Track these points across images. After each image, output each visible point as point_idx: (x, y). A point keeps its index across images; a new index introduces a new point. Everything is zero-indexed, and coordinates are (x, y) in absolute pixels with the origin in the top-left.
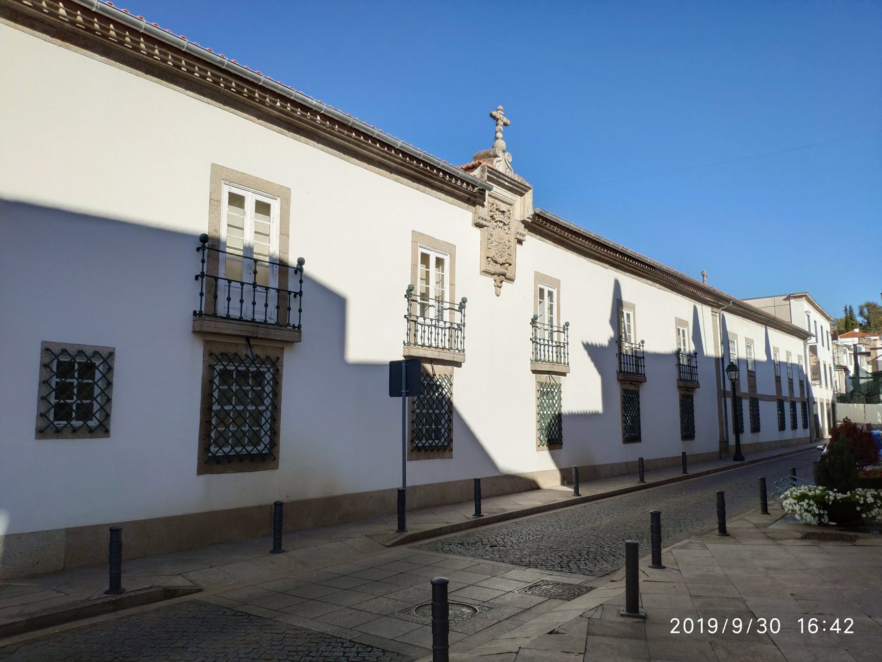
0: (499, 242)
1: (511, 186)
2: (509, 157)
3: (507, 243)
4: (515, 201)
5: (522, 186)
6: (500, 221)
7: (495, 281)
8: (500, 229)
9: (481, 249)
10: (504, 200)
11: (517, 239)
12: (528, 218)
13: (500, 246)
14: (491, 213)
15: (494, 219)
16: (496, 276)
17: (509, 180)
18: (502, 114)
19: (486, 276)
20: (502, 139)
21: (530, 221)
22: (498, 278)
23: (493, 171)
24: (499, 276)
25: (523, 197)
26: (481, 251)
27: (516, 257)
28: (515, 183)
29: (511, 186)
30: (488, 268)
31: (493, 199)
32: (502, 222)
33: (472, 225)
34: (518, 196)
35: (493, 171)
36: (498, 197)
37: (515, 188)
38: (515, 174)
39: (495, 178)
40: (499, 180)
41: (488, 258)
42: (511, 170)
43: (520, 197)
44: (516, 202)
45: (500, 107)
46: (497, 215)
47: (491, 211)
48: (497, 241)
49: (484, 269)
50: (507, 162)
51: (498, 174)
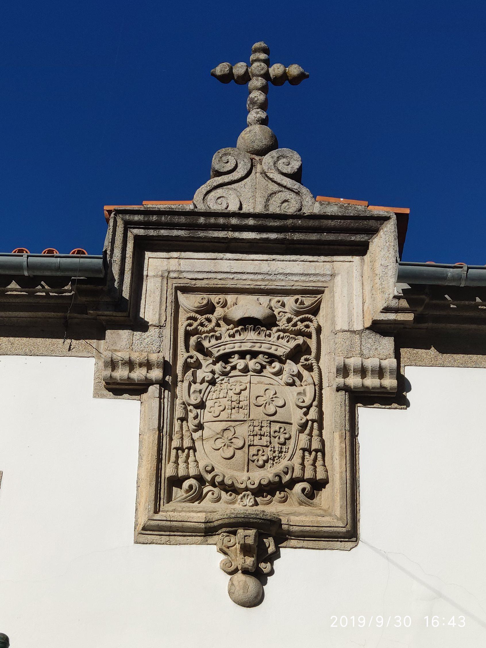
0: (233, 417)
1: (273, 236)
4: (333, 275)
5: (332, 223)
6: (242, 355)
10: (262, 285)
11: (345, 388)
15: (206, 353)
17: (251, 222)
21: (410, 317)
23: (154, 218)
28: (290, 222)
29: (273, 236)
32: (254, 354)
33: (97, 395)
34: (349, 258)
35: (154, 218)
36: (229, 284)
37: (297, 236)
39: (181, 233)
40: (202, 234)
42: (298, 193)
43: (356, 259)
44: (338, 279)
48: (224, 416)
50: (279, 178)
51: (183, 220)
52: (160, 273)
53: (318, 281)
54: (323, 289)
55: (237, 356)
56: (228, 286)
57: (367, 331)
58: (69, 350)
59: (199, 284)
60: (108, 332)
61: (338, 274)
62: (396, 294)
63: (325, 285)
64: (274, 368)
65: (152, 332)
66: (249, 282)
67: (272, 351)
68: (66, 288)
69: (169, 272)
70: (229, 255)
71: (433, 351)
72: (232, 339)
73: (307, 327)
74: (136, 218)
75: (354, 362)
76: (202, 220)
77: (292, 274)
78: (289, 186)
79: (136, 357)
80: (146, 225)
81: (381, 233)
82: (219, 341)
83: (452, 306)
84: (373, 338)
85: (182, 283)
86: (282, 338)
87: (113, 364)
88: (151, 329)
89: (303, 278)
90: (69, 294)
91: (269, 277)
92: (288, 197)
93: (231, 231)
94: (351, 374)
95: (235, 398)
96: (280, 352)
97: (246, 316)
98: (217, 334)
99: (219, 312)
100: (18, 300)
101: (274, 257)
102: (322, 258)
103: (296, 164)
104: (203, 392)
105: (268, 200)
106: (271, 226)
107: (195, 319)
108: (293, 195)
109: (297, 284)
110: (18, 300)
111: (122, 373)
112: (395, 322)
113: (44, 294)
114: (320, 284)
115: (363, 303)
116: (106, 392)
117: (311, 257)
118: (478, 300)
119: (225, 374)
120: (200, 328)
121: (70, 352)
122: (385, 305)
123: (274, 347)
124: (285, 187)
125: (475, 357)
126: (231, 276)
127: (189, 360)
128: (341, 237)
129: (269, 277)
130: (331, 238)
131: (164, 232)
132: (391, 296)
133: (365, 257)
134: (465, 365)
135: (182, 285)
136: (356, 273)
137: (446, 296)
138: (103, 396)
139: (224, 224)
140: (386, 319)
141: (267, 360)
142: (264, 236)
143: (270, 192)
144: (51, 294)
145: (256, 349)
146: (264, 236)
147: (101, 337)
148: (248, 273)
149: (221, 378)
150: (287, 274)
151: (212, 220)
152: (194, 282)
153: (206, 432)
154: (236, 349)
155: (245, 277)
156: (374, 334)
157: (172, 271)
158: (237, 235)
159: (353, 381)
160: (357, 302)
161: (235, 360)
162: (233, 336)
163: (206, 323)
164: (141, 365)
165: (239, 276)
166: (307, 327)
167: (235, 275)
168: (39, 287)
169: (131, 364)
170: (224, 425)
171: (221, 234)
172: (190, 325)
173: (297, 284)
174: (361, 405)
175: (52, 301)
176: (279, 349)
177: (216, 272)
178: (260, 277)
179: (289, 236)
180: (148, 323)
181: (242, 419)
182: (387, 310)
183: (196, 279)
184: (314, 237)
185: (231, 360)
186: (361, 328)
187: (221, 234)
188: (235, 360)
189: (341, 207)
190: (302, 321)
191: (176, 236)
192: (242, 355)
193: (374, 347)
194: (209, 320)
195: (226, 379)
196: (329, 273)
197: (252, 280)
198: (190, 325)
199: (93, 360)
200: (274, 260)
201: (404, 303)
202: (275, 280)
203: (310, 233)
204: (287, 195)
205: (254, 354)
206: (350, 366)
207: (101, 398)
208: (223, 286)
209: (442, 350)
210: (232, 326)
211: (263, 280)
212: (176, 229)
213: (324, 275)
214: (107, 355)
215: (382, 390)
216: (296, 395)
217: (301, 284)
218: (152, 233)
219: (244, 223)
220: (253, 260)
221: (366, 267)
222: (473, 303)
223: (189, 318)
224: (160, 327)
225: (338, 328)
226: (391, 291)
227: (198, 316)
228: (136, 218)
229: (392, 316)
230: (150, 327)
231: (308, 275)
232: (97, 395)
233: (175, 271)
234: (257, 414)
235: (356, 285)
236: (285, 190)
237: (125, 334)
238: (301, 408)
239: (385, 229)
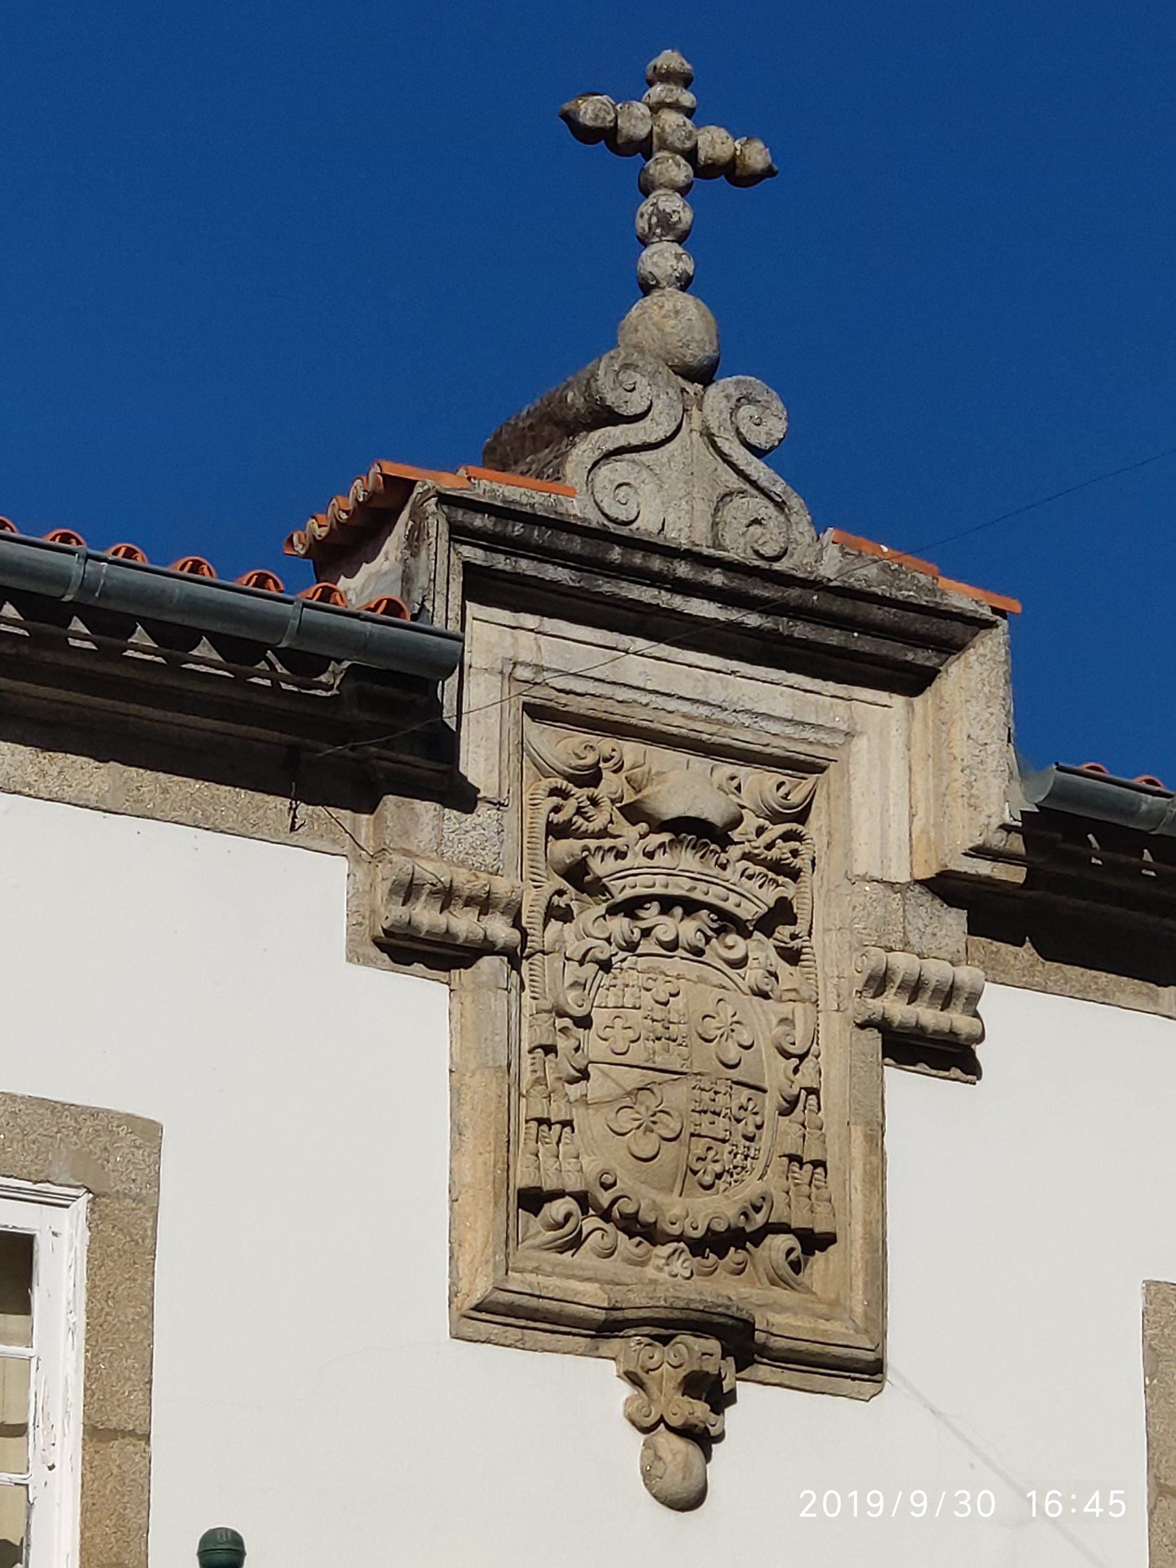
0: (659, 1061)
1: (753, 620)
2: (746, 411)
3: (775, 1074)
5: (878, 614)
6: (667, 904)
7: (633, 1379)
8: (678, 964)
9: (457, 1130)
10: (707, 732)
11: (883, 1026)
12: (980, 852)
13: (678, 1095)
14: (566, 849)
15: (597, 888)
16: (632, 1346)
17: (717, 578)
18: (676, 106)
19: (520, 1345)
20: (685, 283)
21: (1016, 874)
22: (658, 1352)
23: (518, 529)
24: (665, 1340)
25: (929, 693)
26: (455, 1150)
27: (877, 1178)
28: (794, 592)
29: (753, 620)
30: (516, 1282)
31: (580, 738)
32: (691, 907)
33: (354, 956)
34: (882, 696)
35: (518, 529)
36: (638, 717)
37: (801, 630)
38: (819, 526)
40: (606, 587)
41: (533, 1200)
42: (780, 506)
43: (898, 701)
44: (860, 745)
45: (670, 59)
46: (635, 859)
47: (557, 831)
48: (637, 1054)
49: (480, 1288)
52: (498, 665)
53: (819, 743)
54: (825, 763)
55: (655, 907)
56: (633, 721)
57: (918, 888)
58: (292, 829)
59: (576, 705)
60: (390, 801)
61: (861, 733)
62: (1008, 820)
63: (831, 754)
64: (731, 948)
65: (484, 813)
66: (679, 721)
67: (729, 906)
68: (323, 678)
69: (515, 664)
70: (641, 644)
71: (1027, 952)
72: (646, 861)
73: (795, 853)
74: (479, 521)
75: (903, 963)
76: (616, 554)
77: (770, 717)
78: (764, 483)
79: (463, 879)
80: (492, 542)
81: (971, 655)
82: (622, 864)
83: (1094, 860)
84: (930, 905)
85: (539, 695)
86: (750, 877)
87: (408, 890)
88: (482, 808)
89: (789, 730)
90: (324, 694)
91: (722, 716)
92: (762, 513)
93: (667, 590)
94: (890, 992)
95: (659, 1013)
96: (748, 912)
97: (692, 814)
98: (619, 843)
99: (611, 784)
100: (205, 688)
101: (734, 665)
102: (831, 687)
103: (772, 429)
104: (588, 987)
105: (717, 510)
106: (756, 597)
107: (565, 795)
108: (772, 510)
109: (776, 741)
110: (205, 688)
111: (426, 916)
112: (988, 881)
113: (268, 683)
114: (821, 752)
115: (912, 816)
116: (374, 951)
117: (808, 679)
118: (1147, 856)
119: (631, 947)
120: (579, 820)
121: (294, 837)
122: (979, 841)
123: (733, 898)
124: (754, 484)
125: (1103, 977)
126: (644, 699)
127: (556, 898)
128: (887, 648)
129: (722, 716)
130: (867, 649)
131: (526, 566)
132: (995, 822)
133: (917, 701)
134: (1083, 995)
135: (538, 701)
136: (896, 740)
137: (1090, 836)
138: (366, 961)
139: (660, 573)
140: (973, 872)
141: (715, 926)
142: (733, 615)
143: (722, 491)
144: (283, 685)
145: (698, 895)
146: (733, 615)
147: (366, 803)
148: (680, 698)
149: (622, 955)
150: (758, 715)
151: (638, 559)
152: (564, 699)
153: (596, 1087)
154: (658, 890)
155: (672, 704)
156: (929, 897)
157: (522, 664)
158: (678, 602)
159: (896, 1008)
160: (899, 811)
161: (651, 914)
162: (650, 855)
163: (591, 811)
164: (469, 902)
165: (660, 701)
166: (795, 853)
167: (653, 697)
168: (263, 665)
169: (447, 896)
170: (633, 1078)
171: (647, 595)
172: (557, 809)
173: (776, 741)
174: (892, 1062)
175: (283, 704)
176: (744, 902)
177: (614, 683)
178: (704, 711)
179: (783, 625)
180: (478, 791)
181: (678, 1068)
182: (980, 852)
183: (568, 692)
184: (834, 638)
185: (642, 913)
186: (905, 878)
187: (647, 595)
188: (651, 914)
189: (885, 569)
190: (786, 837)
191: (551, 581)
192: (667, 904)
193: (929, 930)
194: (594, 802)
195: (632, 959)
196: (844, 727)
197: (685, 716)
198: (557, 809)
199: (343, 865)
200: (733, 672)
201: (1017, 844)
202: (730, 725)
203: (826, 625)
204: (765, 509)
205: (691, 907)
206: (893, 973)
207: (364, 964)
208: (624, 720)
209: (1047, 954)
210: (643, 827)
211: (707, 719)
212: (553, 564)
213: (833, 730)
214: (400, 866)
215: (951, 1038)
216: (775, 1021)
217: (784, 744)
218: (501, 562)
219: (703, 578)
220: (689, 666)
221: (917, 727)
222: (1134, 860)
223: (554, 792)
224: (499, 805)
225: (860, 869)
226: (994, 809)
227: (575, 790)
228: (479, 521)
229: (984, 868)
230: (479, 804)
231: (803, 724)
232: (354, 956)
233: (528, 665)
234: (704, 1058)
235: (897, 768)
236: (755, 492)
237: (426, 810)
238: (787, 1055)
239: (981, 650)
